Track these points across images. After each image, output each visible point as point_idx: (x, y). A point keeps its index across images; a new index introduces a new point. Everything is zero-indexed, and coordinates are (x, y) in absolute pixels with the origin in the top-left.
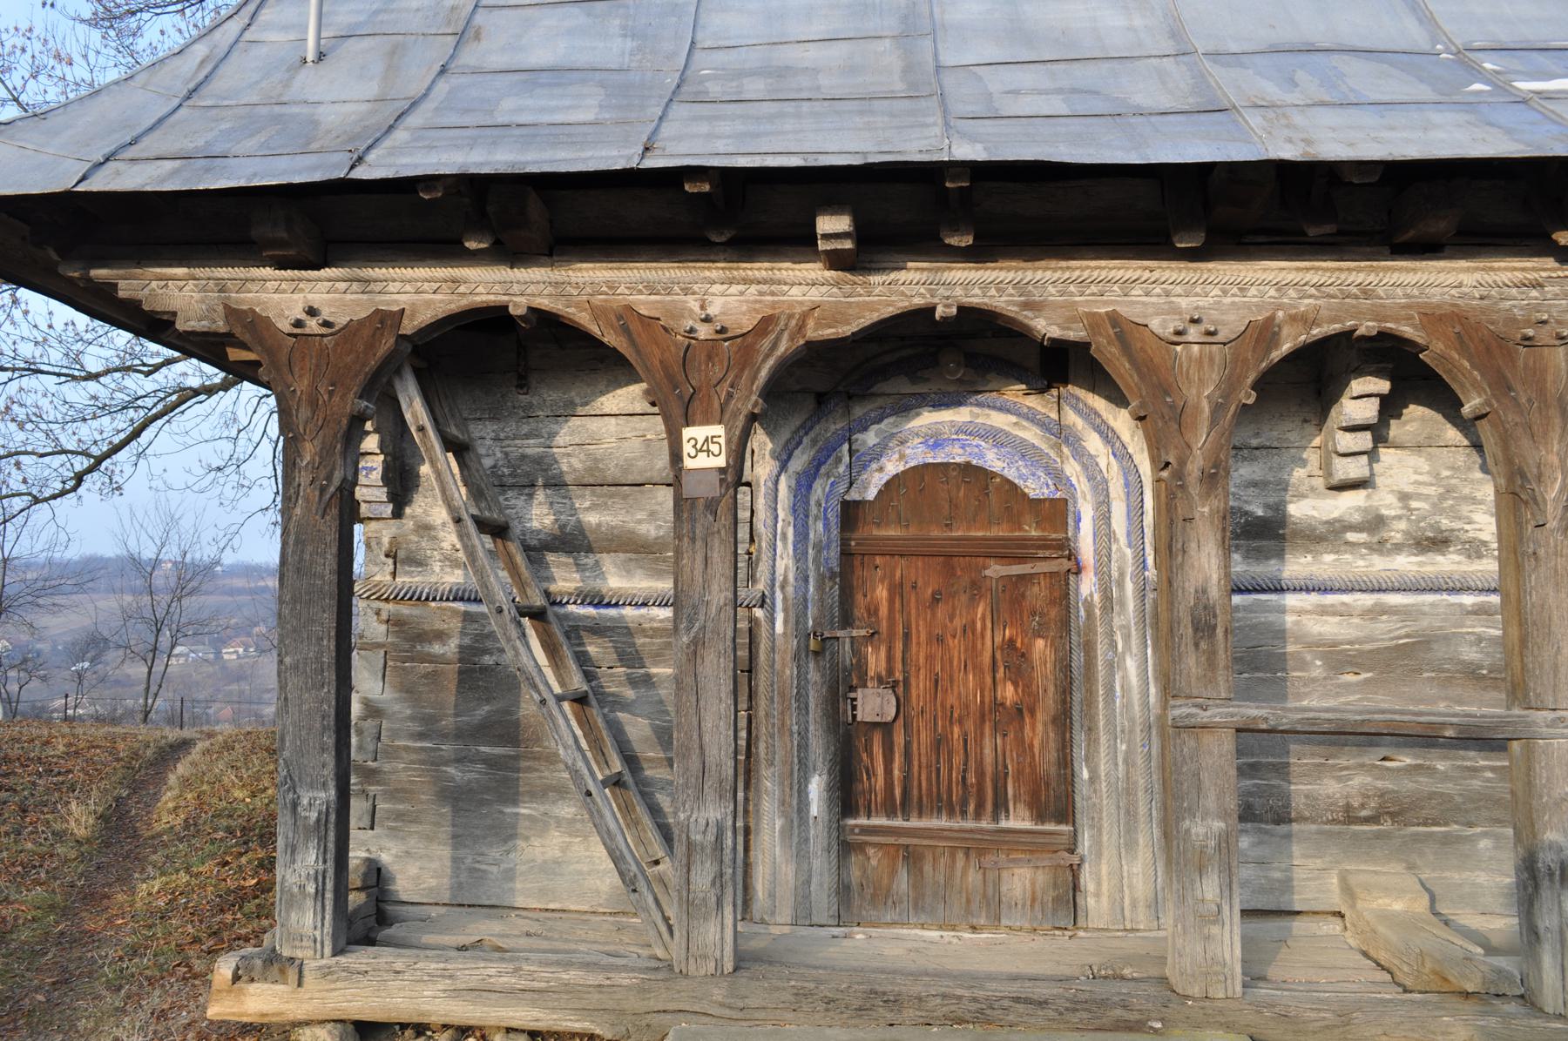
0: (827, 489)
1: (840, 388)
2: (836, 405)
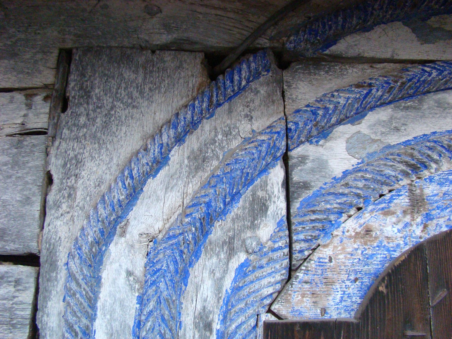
0: (228, 284)
1: (264, 42)
2: (257, 75)
